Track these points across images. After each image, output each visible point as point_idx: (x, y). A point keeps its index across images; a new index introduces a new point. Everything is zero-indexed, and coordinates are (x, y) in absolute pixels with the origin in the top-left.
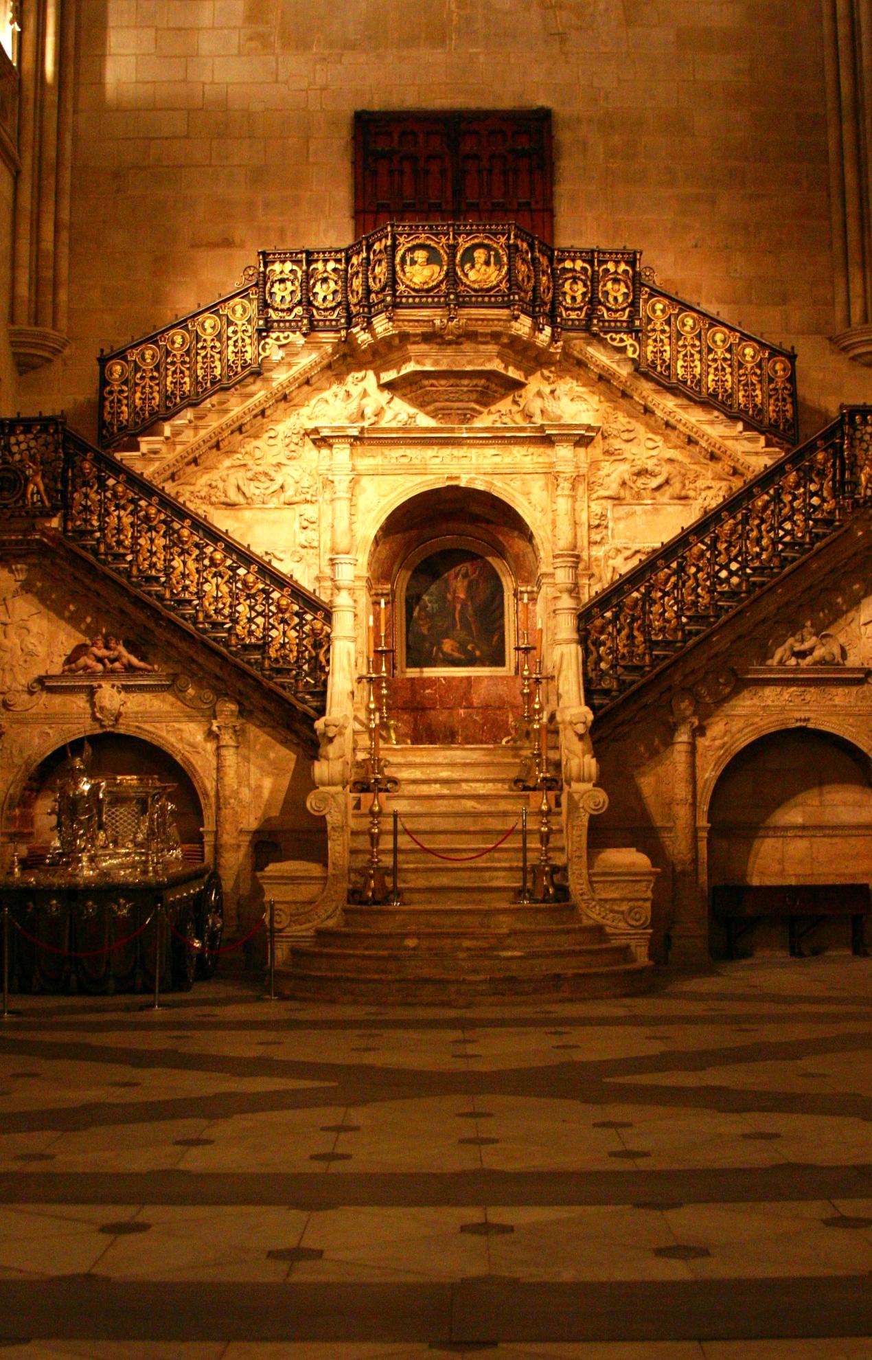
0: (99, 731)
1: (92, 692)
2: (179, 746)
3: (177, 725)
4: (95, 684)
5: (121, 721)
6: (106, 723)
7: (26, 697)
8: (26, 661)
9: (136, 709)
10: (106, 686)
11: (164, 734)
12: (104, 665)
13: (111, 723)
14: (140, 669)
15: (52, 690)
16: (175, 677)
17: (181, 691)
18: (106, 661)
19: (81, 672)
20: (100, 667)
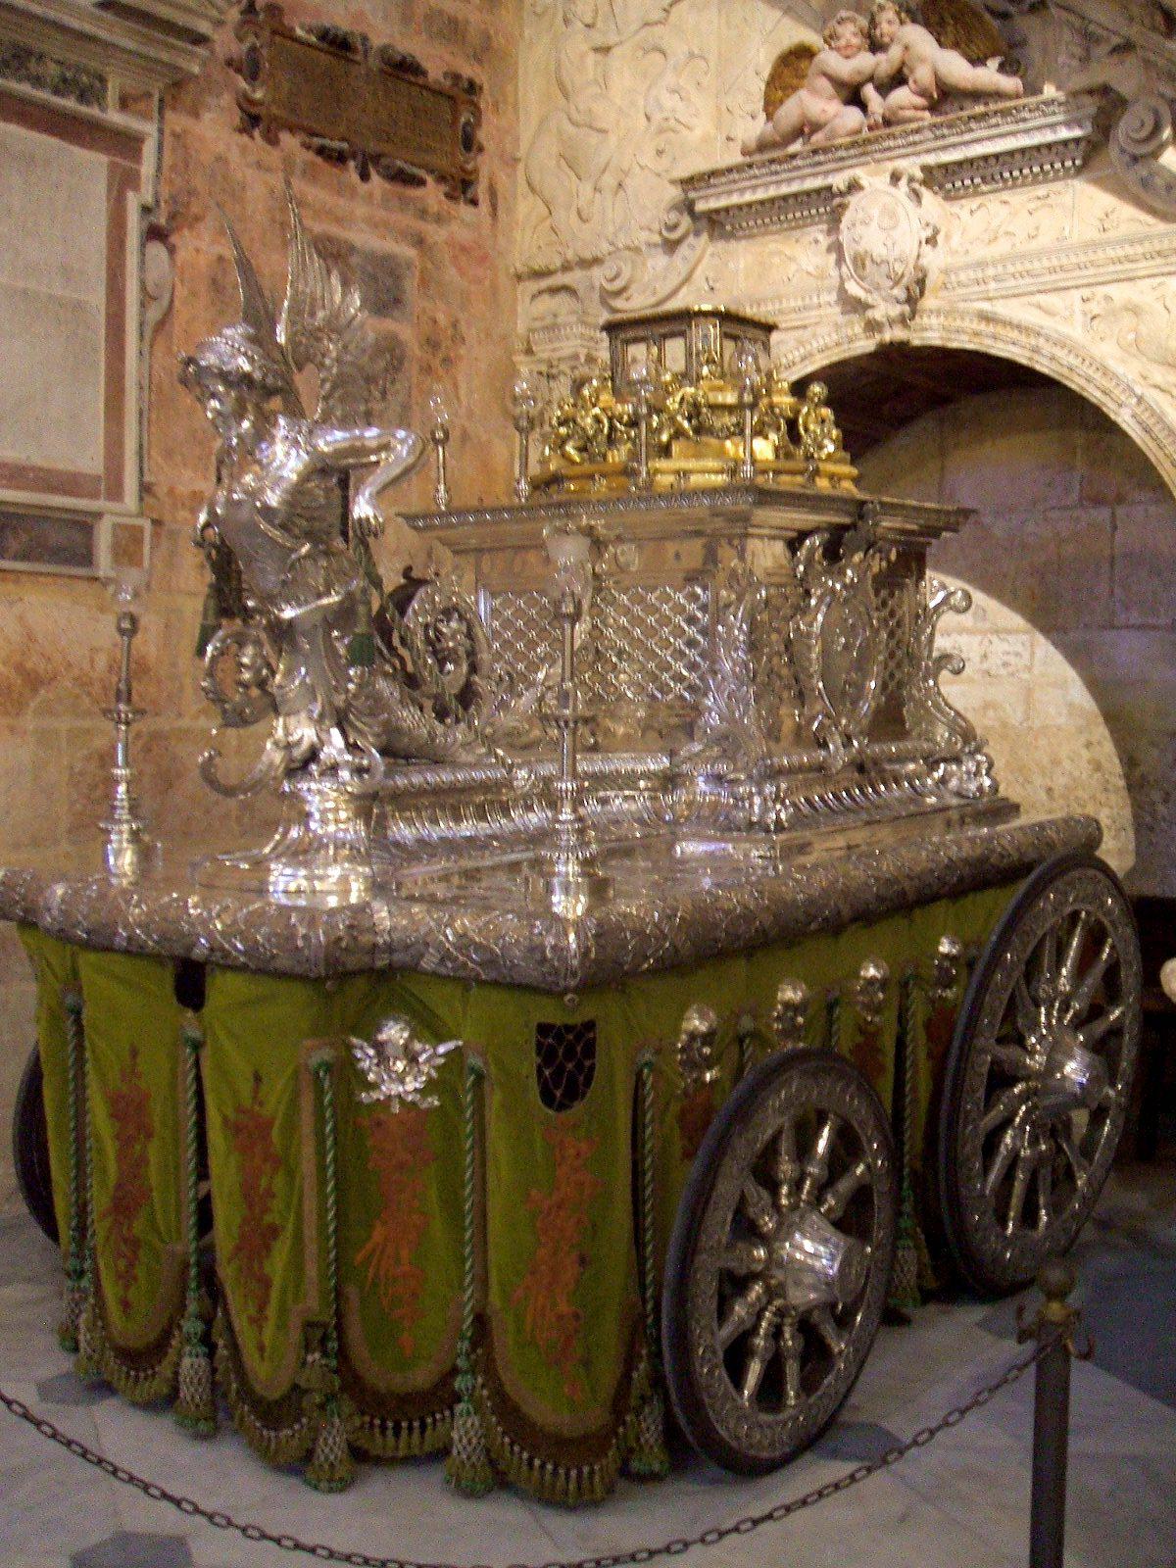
0: (866, 345)
1: (829, 205)
2: (1128, 370)
3: (1120, 293)
4: (839, 181)
5: (929, 302)
6: (877, 314)
7: (659, 261)
8: (660, 153)
9: (981, 252)
10: (873, 178)
11: (1076, 332)
12: (863, 106)
13: (895, 311)
14: (977, 95)
15: (716, 224)
16: (1107, 107)
17: (1135, 159)
18: (869, 91)
19: (796, 147)
20: (852, 116)
